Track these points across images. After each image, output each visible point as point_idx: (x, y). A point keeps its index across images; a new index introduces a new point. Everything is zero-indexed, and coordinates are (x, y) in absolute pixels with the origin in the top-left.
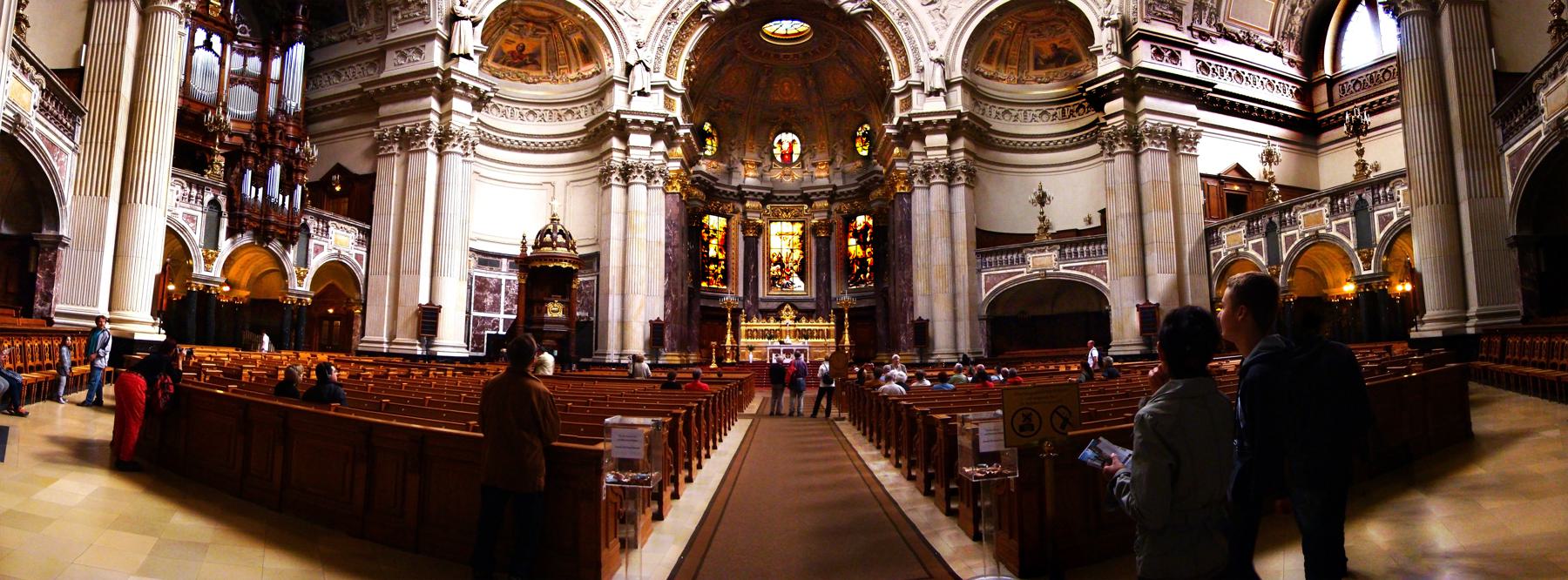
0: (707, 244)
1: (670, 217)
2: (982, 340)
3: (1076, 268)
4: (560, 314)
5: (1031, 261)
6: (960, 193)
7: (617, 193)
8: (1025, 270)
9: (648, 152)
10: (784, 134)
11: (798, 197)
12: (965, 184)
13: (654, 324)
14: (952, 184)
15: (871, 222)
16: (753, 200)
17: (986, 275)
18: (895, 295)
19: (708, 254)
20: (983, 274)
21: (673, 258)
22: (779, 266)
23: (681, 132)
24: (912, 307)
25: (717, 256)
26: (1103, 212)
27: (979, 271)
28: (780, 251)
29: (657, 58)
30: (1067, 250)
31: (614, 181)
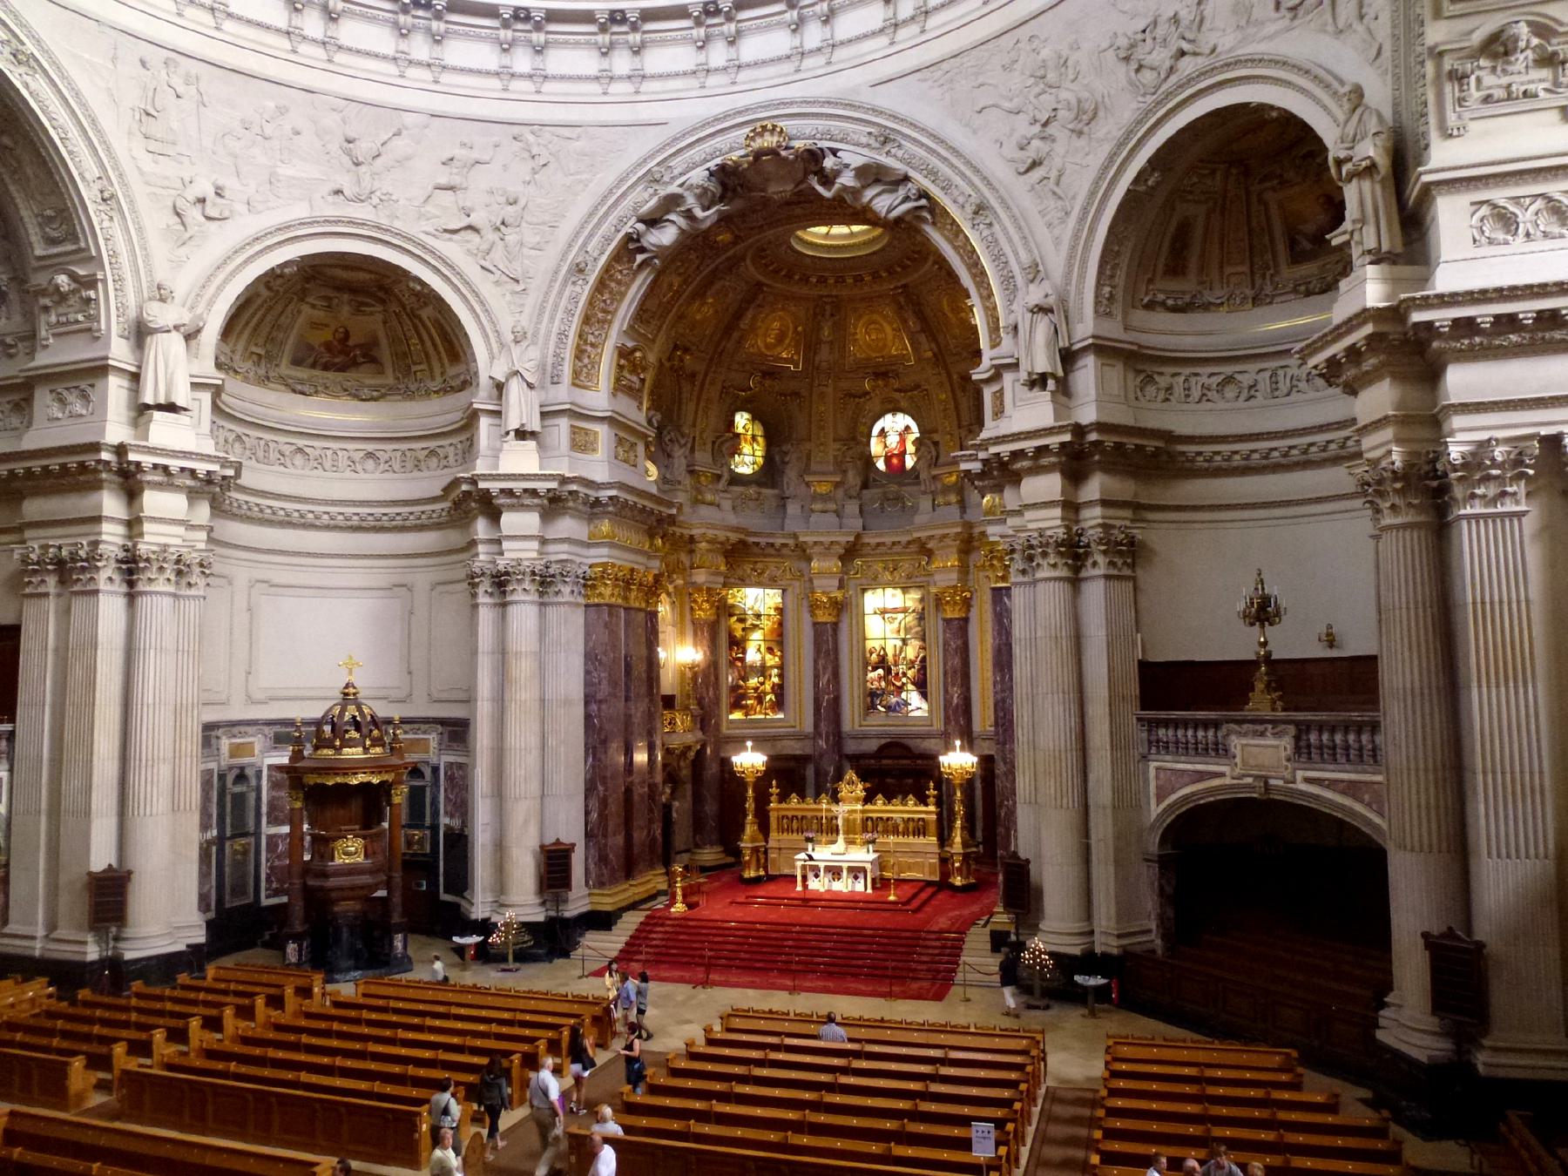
0: (738, 644)
1: (594, 648)
3: (1332, 784)
4: (360, 859)
5: (1238, 752)
6: (1095, 593)
7: (486, 616)
11: (909, 543)
12: (1107, 577)
13: (549, 851)
14: (1083, 574)
16: (825, 555)
17: (1157, 769)
19: (742, 660)
20: (1153, 765)
21: (601, 721)
22: (880, 671)
23: (605, 494)
25: (763, 659)
27: (1145, 758)
28: (882, 642)
29: (556, 355)
31: (483, 599)
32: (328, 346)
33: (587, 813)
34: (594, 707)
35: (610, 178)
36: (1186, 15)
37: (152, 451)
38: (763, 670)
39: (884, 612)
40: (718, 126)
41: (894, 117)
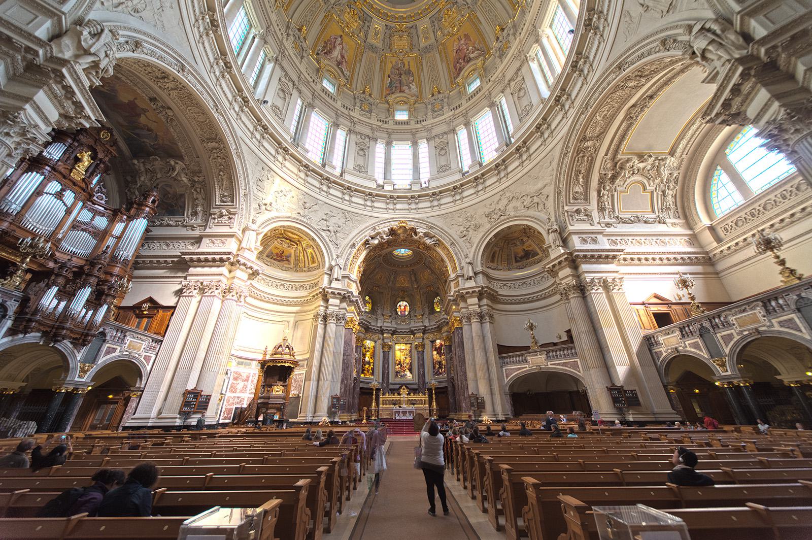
0: (364, 355)
2: (508, 407)
3: (558, 364)
4: (281, 393)
6: (487, 326)
8: (527, 366)
9: (338, 308)
10: (402, 302)
15: (443, 343)
18: (458, 380)
20: (504, 368)
24: (467, 387)
26: (569, 332)
27: (502, 367)
30: (551, 354)
32: (277, 254)
33: (341, 389)
34: (345, 357)
35: (363, 227)
36: (502, 209)
37: (245, 258)
38: (369, 363)
39: (400, 350)
40: (392, 220)
41: (432, 224)
